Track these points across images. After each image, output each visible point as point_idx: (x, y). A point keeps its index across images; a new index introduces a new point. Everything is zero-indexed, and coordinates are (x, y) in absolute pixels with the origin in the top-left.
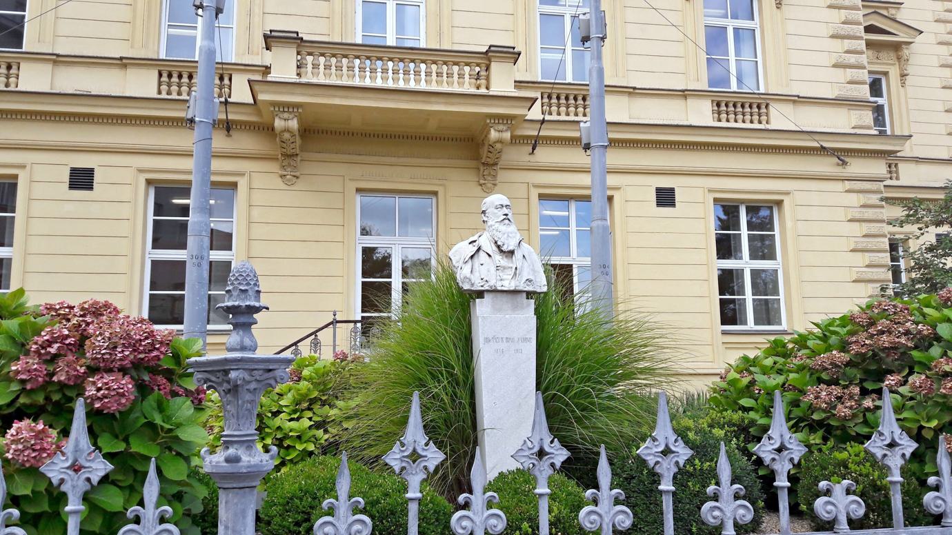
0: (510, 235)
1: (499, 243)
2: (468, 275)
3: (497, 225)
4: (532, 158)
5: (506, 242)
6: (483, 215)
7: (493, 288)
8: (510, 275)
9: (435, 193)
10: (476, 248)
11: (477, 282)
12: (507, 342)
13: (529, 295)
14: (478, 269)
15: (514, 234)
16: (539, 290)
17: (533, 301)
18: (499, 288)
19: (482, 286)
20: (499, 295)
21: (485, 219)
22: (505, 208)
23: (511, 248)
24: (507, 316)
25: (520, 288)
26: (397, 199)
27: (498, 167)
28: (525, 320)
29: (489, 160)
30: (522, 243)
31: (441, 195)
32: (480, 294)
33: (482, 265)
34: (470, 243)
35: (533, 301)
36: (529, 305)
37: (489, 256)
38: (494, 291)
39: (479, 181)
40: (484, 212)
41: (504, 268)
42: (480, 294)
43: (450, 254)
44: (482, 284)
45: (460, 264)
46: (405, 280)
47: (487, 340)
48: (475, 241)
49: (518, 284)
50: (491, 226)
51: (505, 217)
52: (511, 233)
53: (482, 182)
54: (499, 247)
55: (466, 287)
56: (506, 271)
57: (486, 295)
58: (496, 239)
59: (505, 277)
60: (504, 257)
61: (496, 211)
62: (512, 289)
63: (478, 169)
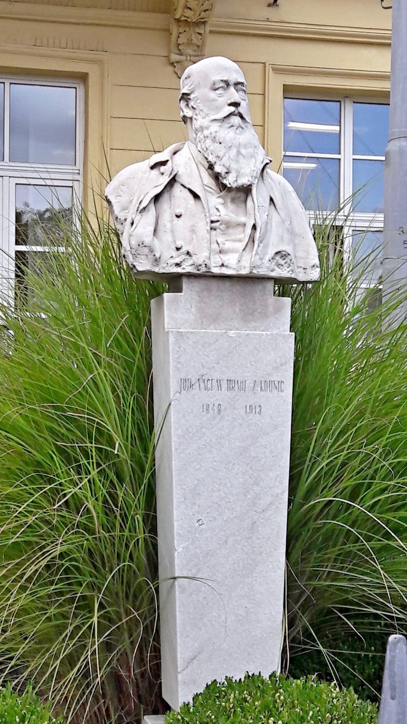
0: (243, 151)
1: (218, 169)
2: (148, 239)
3: (215, 127)
4: (272, 13)
5: (234, 166)
6: (183, 104)
7: (203, 269)
8: (240, 241)
9: (83, 78)
10: (166, 180)
11: (166, 256)
12: (230, 389)
13: (283, 286)
14: (169, 226)
15: (251, 150)
16: (301, 277)
17: (288, 301)
18: (216, 270)
19: (178, 265)
20: (214, 284)
21: (188, 113)
22: (232, 89)
23: (244, 181)
24: (232, 333)
25: (262, 271)
26: (7, 85)
27: (208, 28)
28: (269, 343)
29: (188, 13)
30: (268, 170)
31: (92, 80)
32: (174, 282)
33: (178, 216)
34: (152, 168)
35: (288, 301)
36: (278, 310)
37: (196, 196)
38: (205, 276)
39: (168, 57)
40: (185, 97)
41: (228, 225)
42: (174, 282)
43: (109, 191)
44: (178, 260)
45: (131, 214)
46: (22, 248)
47: (186, 384)
48: (164, 163)
49: (259, 263)
50: (202, 129)
51: (232, 109)
52: (245, 146)
53: (175, 57)
54: (217, 177)
55: (143, 265)
56: (231, 231)
57: (185, 284)
58: (212, 159)
59: (228, 245)
60: (229, 200)
61: (213, 95)
62: (244, 272)
63: (168, 31)
